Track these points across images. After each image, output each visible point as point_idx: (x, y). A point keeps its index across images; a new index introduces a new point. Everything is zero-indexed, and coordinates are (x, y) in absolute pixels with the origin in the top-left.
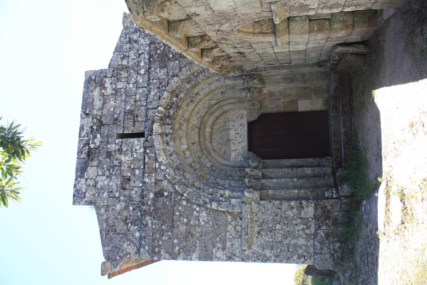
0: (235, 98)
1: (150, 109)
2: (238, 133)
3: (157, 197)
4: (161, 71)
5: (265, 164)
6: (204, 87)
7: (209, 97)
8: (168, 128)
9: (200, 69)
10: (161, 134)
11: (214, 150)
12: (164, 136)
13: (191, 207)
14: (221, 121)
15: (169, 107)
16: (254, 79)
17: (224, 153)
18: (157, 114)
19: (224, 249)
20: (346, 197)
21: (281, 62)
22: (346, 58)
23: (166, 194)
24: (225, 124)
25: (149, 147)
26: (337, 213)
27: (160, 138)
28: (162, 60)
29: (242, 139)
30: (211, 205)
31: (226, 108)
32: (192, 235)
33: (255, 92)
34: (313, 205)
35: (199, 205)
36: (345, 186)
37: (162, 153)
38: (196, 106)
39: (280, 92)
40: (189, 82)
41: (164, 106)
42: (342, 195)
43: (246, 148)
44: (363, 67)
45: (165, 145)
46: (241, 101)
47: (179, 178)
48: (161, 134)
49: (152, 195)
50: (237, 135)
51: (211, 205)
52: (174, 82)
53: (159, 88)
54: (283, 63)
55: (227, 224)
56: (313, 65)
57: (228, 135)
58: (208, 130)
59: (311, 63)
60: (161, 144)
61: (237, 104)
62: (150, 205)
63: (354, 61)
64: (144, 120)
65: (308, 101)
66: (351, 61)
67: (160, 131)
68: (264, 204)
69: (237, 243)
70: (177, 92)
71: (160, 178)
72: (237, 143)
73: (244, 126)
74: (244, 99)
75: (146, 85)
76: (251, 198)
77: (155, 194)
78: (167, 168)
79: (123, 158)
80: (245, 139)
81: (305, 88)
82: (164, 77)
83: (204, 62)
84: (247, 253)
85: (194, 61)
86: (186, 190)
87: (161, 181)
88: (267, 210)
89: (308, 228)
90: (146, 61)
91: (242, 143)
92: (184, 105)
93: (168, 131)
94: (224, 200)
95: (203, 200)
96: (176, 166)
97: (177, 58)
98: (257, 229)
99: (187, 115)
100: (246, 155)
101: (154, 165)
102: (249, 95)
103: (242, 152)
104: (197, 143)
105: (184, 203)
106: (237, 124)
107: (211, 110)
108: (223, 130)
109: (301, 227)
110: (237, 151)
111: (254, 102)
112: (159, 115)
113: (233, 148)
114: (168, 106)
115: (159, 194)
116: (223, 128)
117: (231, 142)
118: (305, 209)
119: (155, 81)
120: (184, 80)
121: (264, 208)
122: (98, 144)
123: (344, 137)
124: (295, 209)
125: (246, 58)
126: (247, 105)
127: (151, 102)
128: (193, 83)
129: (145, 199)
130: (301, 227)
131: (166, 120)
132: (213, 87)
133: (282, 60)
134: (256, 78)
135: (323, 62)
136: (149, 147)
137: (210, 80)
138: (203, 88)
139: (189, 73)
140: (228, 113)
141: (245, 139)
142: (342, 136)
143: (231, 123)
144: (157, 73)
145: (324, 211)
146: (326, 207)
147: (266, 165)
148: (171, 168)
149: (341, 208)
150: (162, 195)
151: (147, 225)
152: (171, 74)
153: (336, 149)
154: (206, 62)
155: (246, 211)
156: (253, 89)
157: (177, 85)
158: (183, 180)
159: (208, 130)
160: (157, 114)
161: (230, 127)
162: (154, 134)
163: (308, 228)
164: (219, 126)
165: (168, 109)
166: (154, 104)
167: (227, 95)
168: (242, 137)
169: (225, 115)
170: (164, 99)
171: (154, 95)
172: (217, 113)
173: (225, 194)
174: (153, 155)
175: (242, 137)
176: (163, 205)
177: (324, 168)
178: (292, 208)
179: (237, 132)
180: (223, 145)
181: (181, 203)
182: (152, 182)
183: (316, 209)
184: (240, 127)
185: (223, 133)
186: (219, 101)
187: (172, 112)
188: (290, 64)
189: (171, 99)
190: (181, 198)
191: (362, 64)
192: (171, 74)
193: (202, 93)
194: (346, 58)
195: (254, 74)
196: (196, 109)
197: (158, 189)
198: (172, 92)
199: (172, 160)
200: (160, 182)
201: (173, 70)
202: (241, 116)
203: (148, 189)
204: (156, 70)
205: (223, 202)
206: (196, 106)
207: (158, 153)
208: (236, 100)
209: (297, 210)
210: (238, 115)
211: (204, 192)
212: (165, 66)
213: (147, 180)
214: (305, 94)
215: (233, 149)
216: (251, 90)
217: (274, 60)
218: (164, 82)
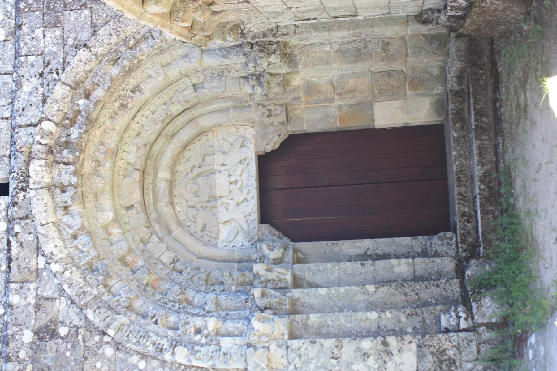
0: (225, 99)
1: (20, 126)
2: (236, 182)
3: (40, 339)
4: (48, 34)
5: (300, 251)
6: (151, 72)
7: (164, 97)
8: (66, 173)
9: (143, 31)
10: (49, 188)
11: (179, 223)
12: (58, 191)
13: (126, 360)
14: (194, 153)
15: (69, 120)
16: (269, 54)
17: (204, 229)
18: (38, 138)
20: (490, 326)
21: (333, 14)
22: (484, 4)
23: (63, 331)
24: (203, 160)
25: (21, 219)
26: (470, 366)
27: (46, 195)
28: (48, 8)
29: (244, 195)
30: (173, 353)
31: (205, 122)
33: (273, 85)
34: (414, 346)
35: (144, 356)
36: (487, 301)
37: (53, 232)
38: (133, 118)
39: (332, 84)
40: (115, 62)
41: (55, 119)
42: (480, 321)
43: (255, 216)
44: (522, 24)
45: (60, 213)
46: (240, 105)
47: (95, 292)
48: (49, 188)
49: (28, 336)
50: (233, 186)
51: (173, 353)
52: (80, 62)
53: (41, 75)
54: (337, 15)
56: (407, 20)
57: (212, 187)
58: (164, 174)
59: (402, 14)
60: (51, 210)
61: (233, 114)
62: (24, 360)
63: (502, 11)
64: (8, 153)
65: (397, 103)
66: (496, 10)
67: (47, 180)
68: (299, 349)
70: (88, 84)
71: (48, 293)
72: (232, 203)
73: (248, 165)
74: (247, 102)
75: (10, 69)
76: (267, 335)
77: (36, 333)
78: (66, 269)
80: (251, 195)
81: (389, 74)
82: (54, 49)
83: (149, 16)
85: (125, 11)
86: (114, 319)
87: (52, 299)
88: (307, 362)
90: (9, 9)
91: (244, 204)
92: (104, 118)
93: (65, 179)
94: (203, 341)
95: (154, 344)
96: (88, 263)
97: (85, 4)
99: (112, 140)
100: (256, 231)
101: (33, 262)
102: (258, 90)
103: (245, 226)
104: (138, 207)
105: (109, 351)
106: (232, 159)
107: (170, 129)
108: (199, 175)
110: (234, 224)
111: (272, 107)
112: (44, 142)
113: (223, 216)
114: (65, 118)
115: (46, 333)
116: (200, 170)
117: (219, 202)
118: (396, 358)
119: (31, 59)
120: (104, 56)
121: (300, 356)
123: (482, 187)
124: (371, 358)
125: (249, 6)
126: (254, 114)
127: (23, 110)
128: (126, 63)
129: (11, 345)
131: (61, 152)
132: (173, 72)
133: (335, 9)
134: (274, 53)
135: (430, 13)
136: (21, 219)
137: (166, 57)
138: (150, 76)
139: (114, 40)
140: (210, 135)
141: (251, 195)
142: (477, 184)
143: (219, 159)
144: (38, 40)
145: (441, 362)
146: (444, 351)
147: (302, 254)
148: (74, 269)
149: (479, 352)
150: (54, 334)
152: (70, 42)
153: (464, 214)
154: (155, 14)
155: (258, 365)
156: (269, 77)
157: (88, 68)
158: (106, 297)
159: (164, 174)
160: (38, 138)
161: (217, 167)
162: (31, 186)
164: (189, 166)
165: (65, 127)
166: (31, 114)
167: (206, 91)
168: (245, 191)
169: (203, 138)
170: (57, 101)
171: (31, 93)
172: (185, 135)
173: (206, 328)
174: (31, 238)
175: (245, 191)
176: (57, 358)
177: (438, 260)
178: (366, 355)
179: (233, 179)
180: (201, 210)
181: (100, 352)
182: (29, 304)
183: (420, 357)
184: (240, 167)
185: (200, 180)
187: (75, 133)
188: (354, 18)
189: (72, 101)
190: (101, 339)
191: (522, 17)
192: (70, 42)
193: (147, 88)
194: (484, 4)
195: (270, 43)
196: (134, 125)
197: (44, 320)
198: (75, 87)
199: (77, 248)
200: (48, 304)
201: (76, 31)
202: (241, 140)
203: (19, 321)
204: (33, 31)
205: (202, 345)
206: (133, 118)
207: (44, 232)
208: (229, 104)
209: (377, 360)
210: (234, 138)
211: (156, 323)
212: (57, 23)
213: (15, 299)
214: (391, 86)
215: (225, 219)
216: (263, 80)
217: (316, 10)
218: (56, 61)
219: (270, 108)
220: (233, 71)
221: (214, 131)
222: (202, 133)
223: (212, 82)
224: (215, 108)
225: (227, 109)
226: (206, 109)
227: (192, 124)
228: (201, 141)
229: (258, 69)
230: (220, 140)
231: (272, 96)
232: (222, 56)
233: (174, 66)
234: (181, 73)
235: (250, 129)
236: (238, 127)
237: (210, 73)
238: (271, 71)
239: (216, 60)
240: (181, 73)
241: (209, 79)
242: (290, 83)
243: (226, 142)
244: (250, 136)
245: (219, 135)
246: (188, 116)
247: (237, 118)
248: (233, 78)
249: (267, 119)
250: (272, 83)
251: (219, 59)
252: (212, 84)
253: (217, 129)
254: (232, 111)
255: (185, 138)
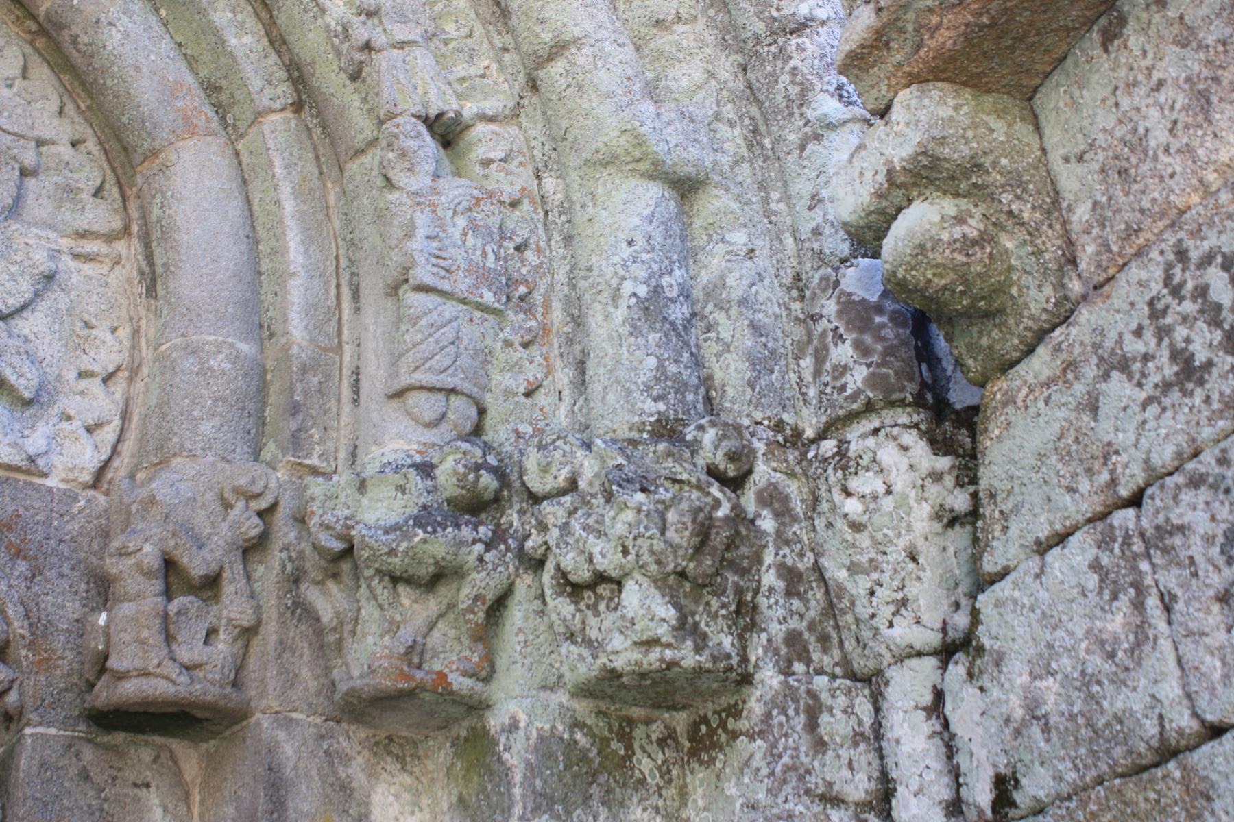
0: (327, 319)
31: (195, 185)
33: (415, 610)
46: (275, 404)
61: (224, 349)
74: (297, 442)
111: (234, 605)
140: (100, 216)
156: (480, 584)
167: (419, 181)
169: (88, 174)
186: (330, 78)
195: (745, 616)
202: (25, 386)
208: (297, 330)
210: (48, 349)
219: (228, 590)
220: (533, 372)
221: (120, 246)
222: (125, 153)
223: (473, 227)
224: (278, 252)
225: (263, 330)
226: (286, 192)
227: (194, 101)
228: (66, 151)
229: (553, 512)
230: (52, 258)
231: (327, 602)
232: (657, 291)
233: (603, 18)
234: (558, 49)
235: (87, 456)
236: (119, 387)
237: (521, 235)
238: (517, 615)
239: (627, 252)
240: (558, 49)
241: (490, 216)
242: (391, 765)
243: (25, 289)
244: (36, 442)
245: (87, 268)
246: (256, 83)
247: (190, 363)
248: (485, 356)
249: (150, 554)
250: (433, 605)
251: (642, 273)
252: (461, 222)
253: (129, 270)
254: (244, 347)
255: (113, 39)
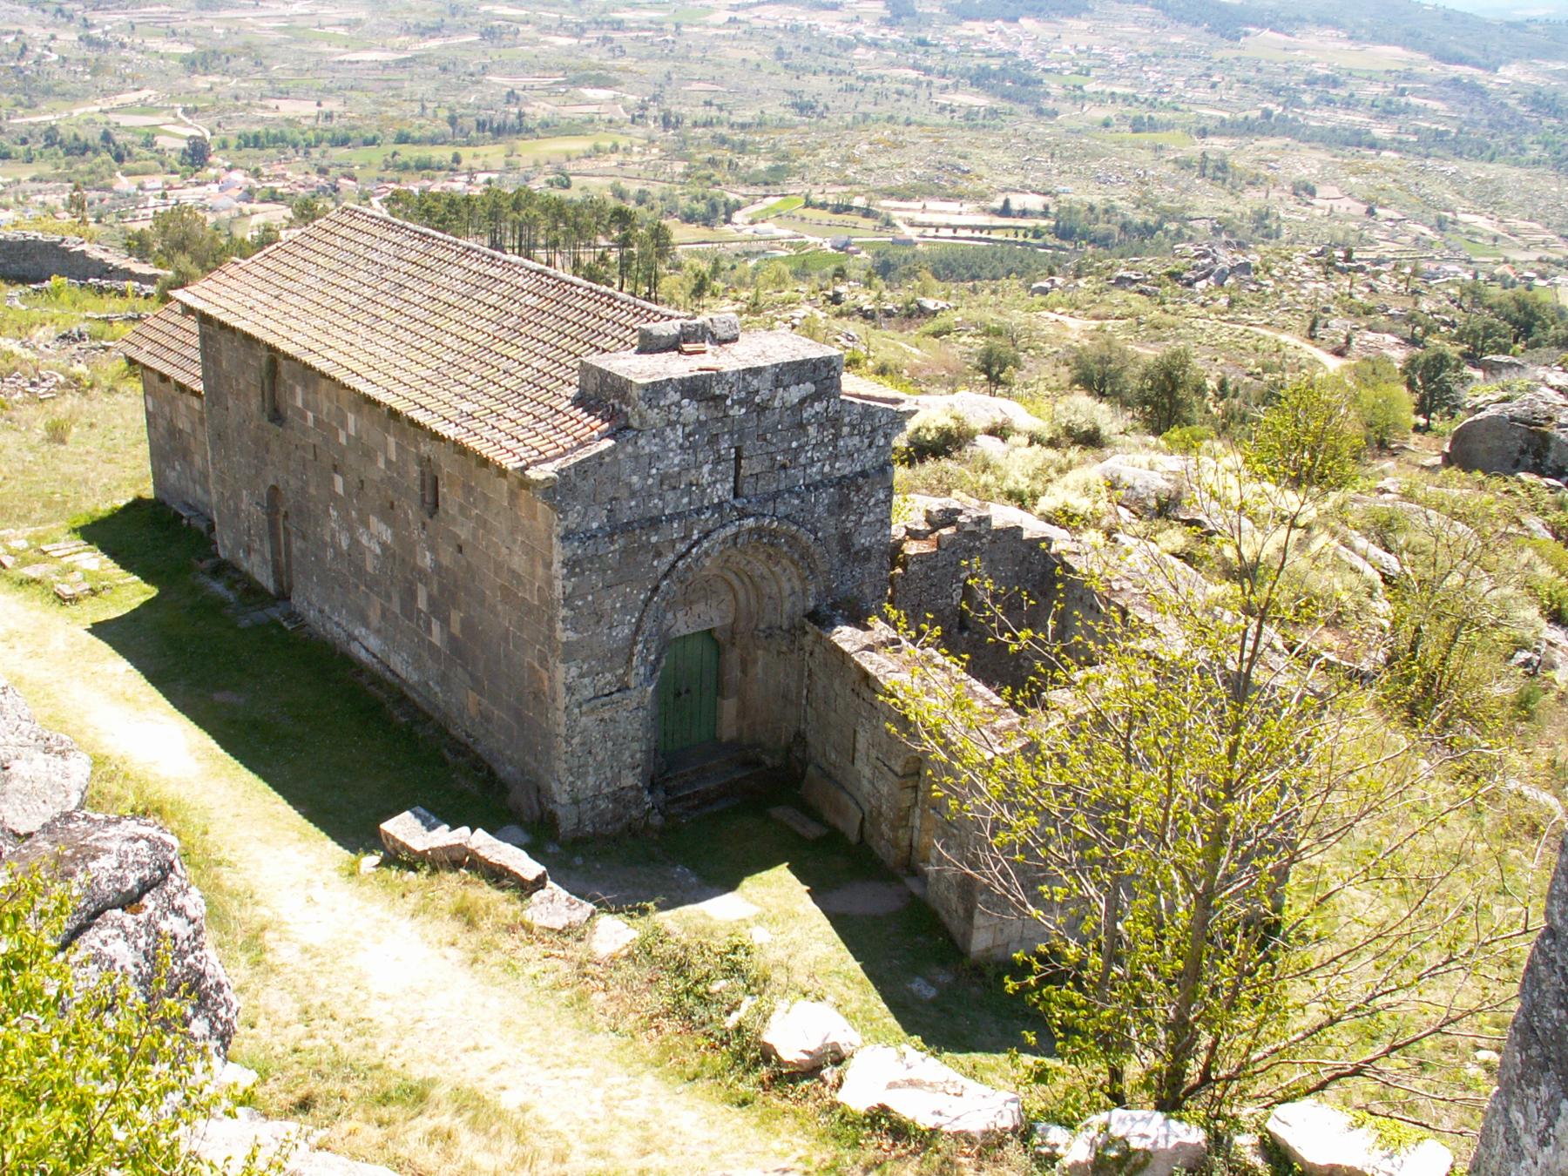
19: (581, 676)
32: (598, 622)
55: (611, 670)
57: (697, 601)
69: (589, 693)
79: (706, 469)
84: (576, 711)
89: (608, 785)
98: (606, 716)
109: (609, 774)
122: (731, 413)
130: (609, 774)
151: (612, 543)
163: (608, 785)
